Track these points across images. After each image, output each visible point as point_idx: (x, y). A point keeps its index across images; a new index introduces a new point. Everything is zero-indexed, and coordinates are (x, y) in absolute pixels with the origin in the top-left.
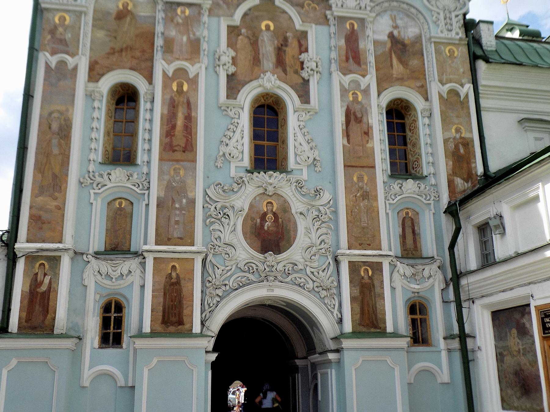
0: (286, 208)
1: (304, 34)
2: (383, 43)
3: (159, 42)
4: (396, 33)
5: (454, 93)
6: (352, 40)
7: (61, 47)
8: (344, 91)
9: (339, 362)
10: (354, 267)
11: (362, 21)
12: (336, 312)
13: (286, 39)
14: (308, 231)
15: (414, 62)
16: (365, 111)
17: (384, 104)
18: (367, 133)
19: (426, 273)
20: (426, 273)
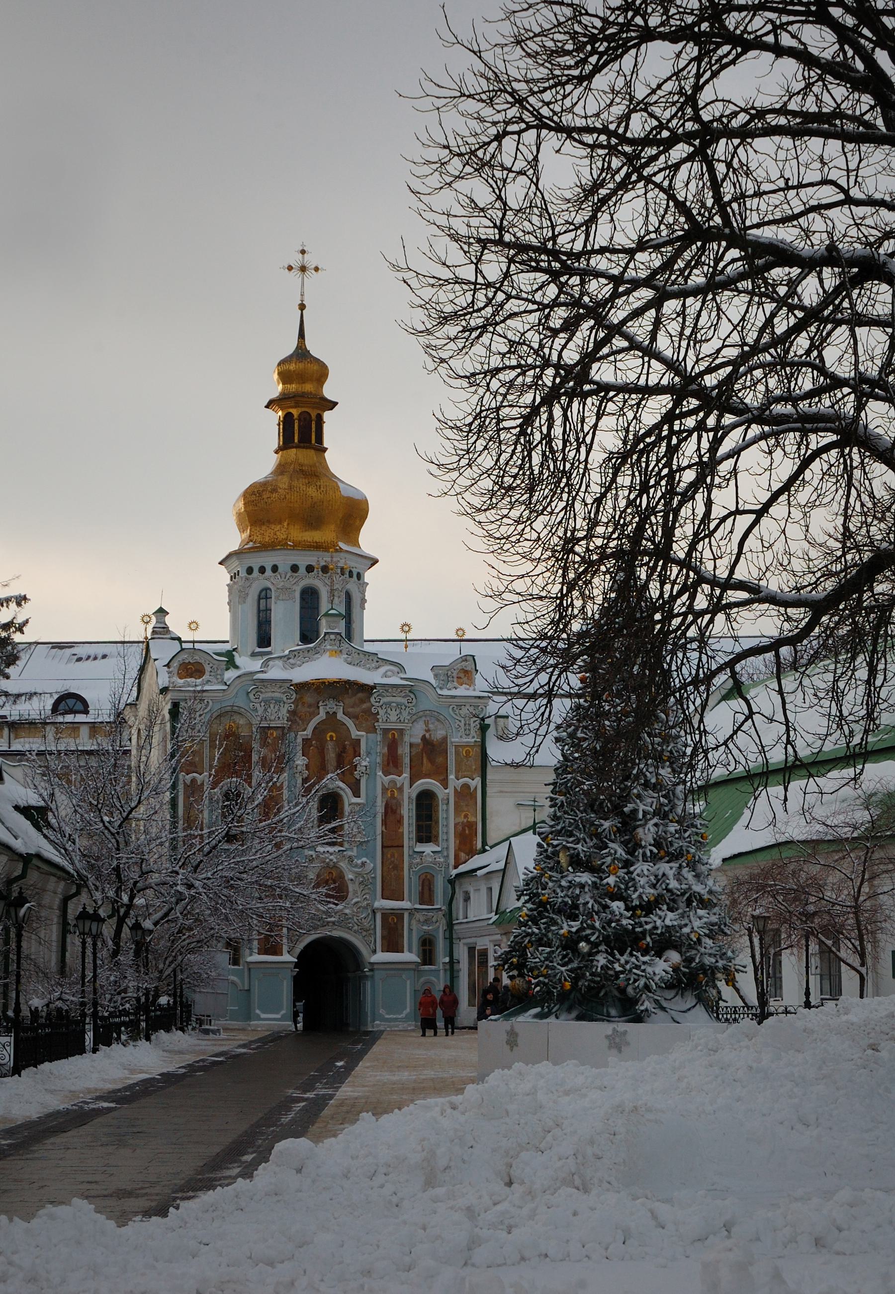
0: (341, 876)
1: (358, 741)
2: (418, 745)
3: (255, 758)
4: (427, 736)
5: (466, 786)
6: (393, 746)
7: (193, 769)
8: (384, 790)
9: (372, 977)
10: (385, 916)
11: (401, 732)
12: (372, 945)
13: (344, 747)
14: (355, 892)
15: (440, 760)
16: (399, 805)
17: (414, 795)
18: (400, 821)
19: (434, 919)
20: (434, 919)
